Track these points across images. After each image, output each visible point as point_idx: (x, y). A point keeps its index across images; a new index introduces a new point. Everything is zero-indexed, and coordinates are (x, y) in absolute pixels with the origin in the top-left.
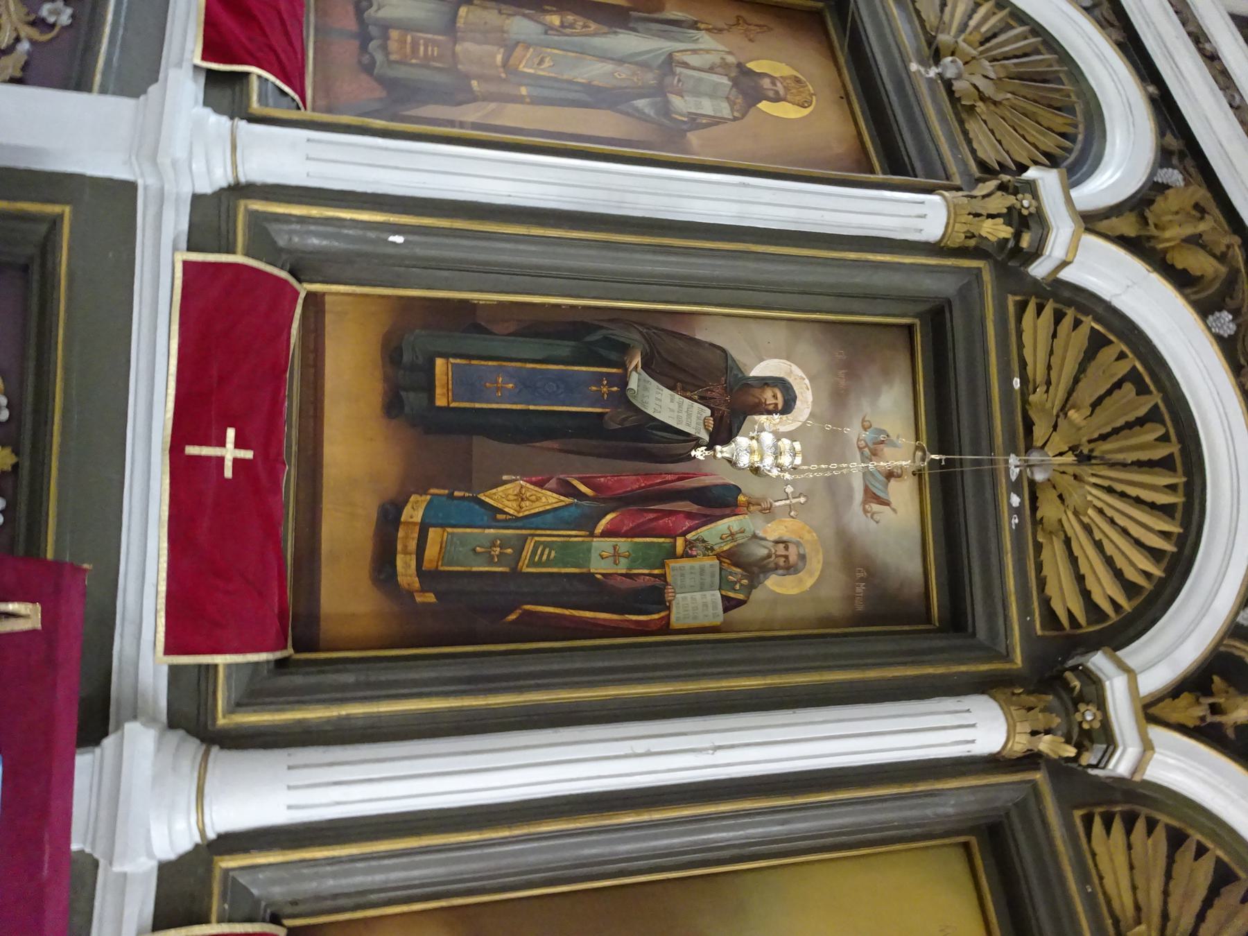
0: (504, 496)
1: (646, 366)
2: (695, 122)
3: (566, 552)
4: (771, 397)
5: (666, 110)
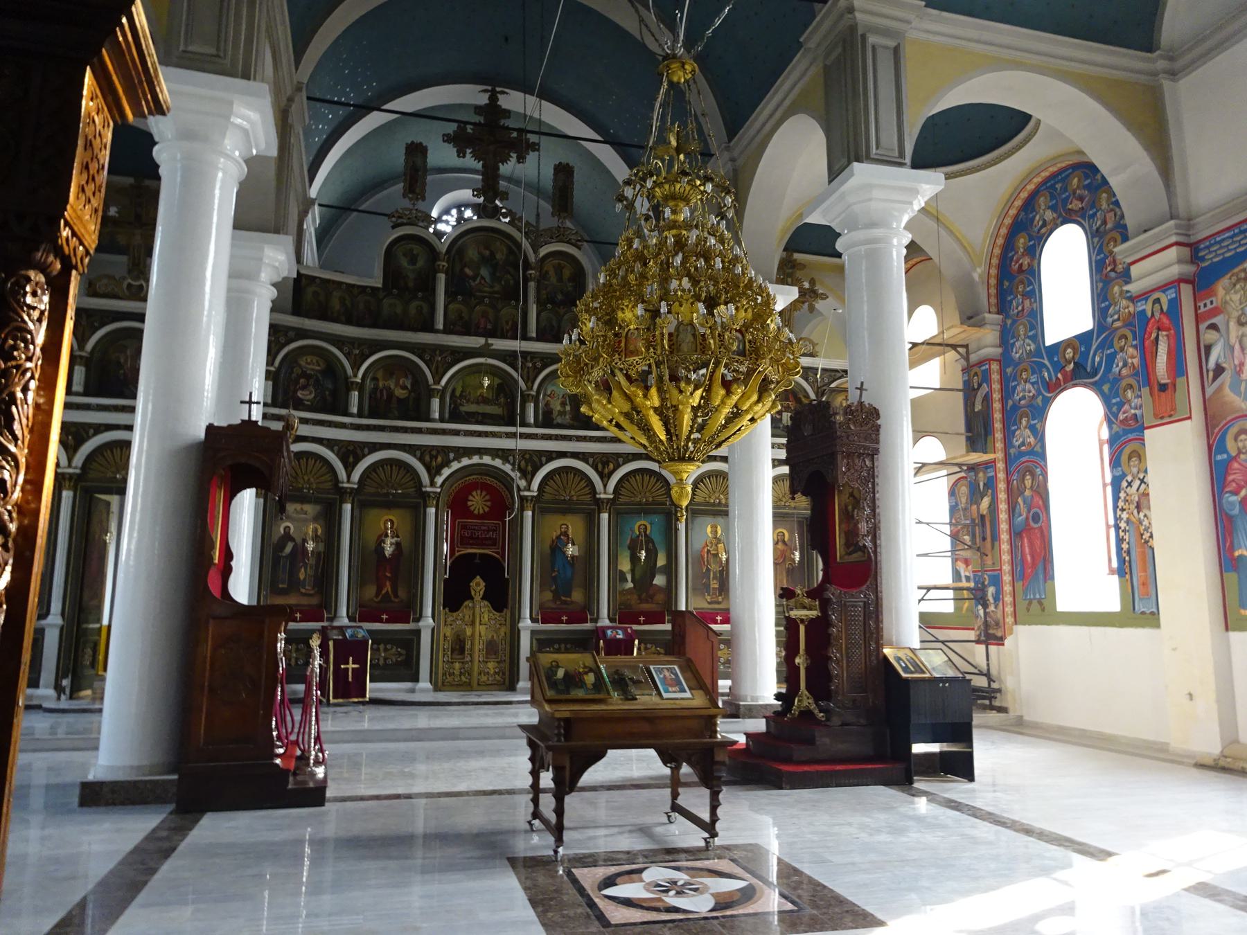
0: (302, 577)
1: (281, 552)
3: (311, 568)
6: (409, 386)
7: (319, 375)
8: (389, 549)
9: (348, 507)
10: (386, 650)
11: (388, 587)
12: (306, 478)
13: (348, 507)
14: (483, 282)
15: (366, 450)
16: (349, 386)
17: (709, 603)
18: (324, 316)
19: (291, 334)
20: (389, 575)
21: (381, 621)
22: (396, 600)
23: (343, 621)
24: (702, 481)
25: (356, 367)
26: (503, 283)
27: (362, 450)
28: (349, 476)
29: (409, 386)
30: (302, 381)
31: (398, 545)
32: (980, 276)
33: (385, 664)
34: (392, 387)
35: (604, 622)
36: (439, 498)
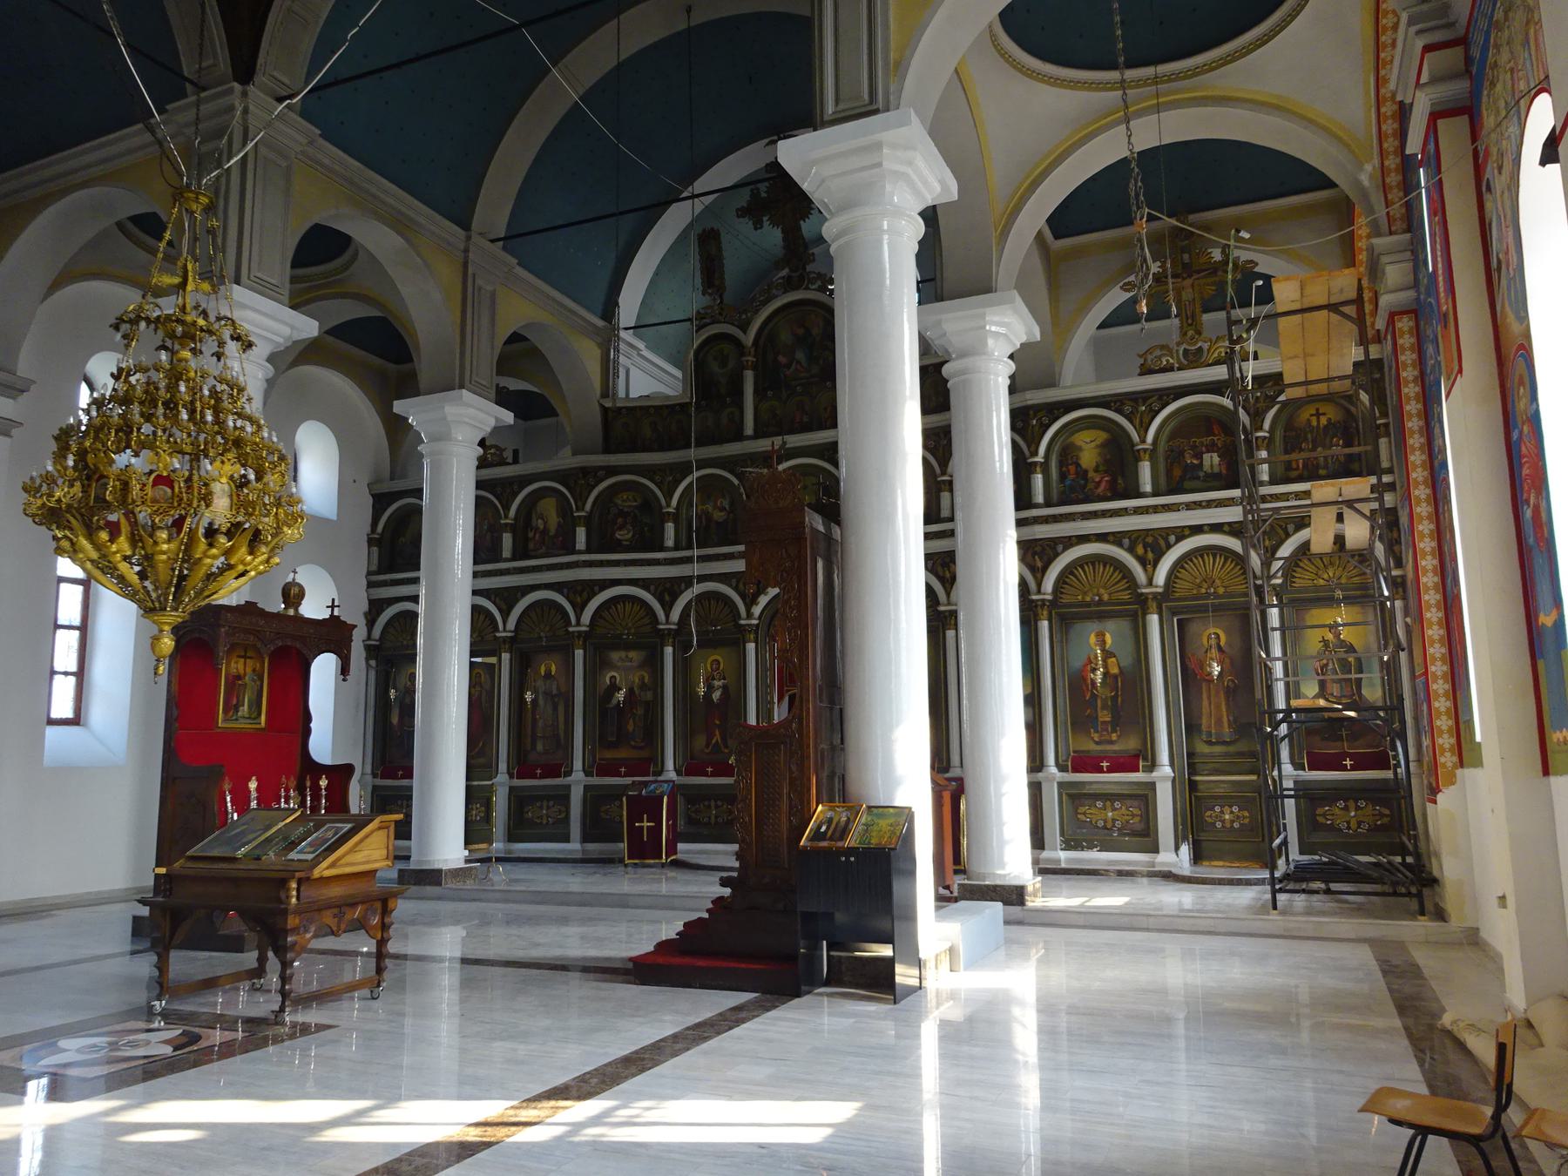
0: (631, 728)
2: (558, 688)
4: (613, 680)
5: (556, 695)
6: (727, 507)
7: (636, 511)
8: (716, 695)
9: (669, 650)
10: (717, 807)
11: (717, 737)
12: (624, 624)
13: (669, 650)
14: (799, 367)
15: (683, 585)
16: (664, 518)
17: (1097, 743)
18: (633, 448)
19: (601, 473)
20: (717, 722)
21: (706, 775)
22: (726, 751)
23: (672, 775)
24: (1072, 573)
25: (669, 496)
26: (821, 362)
27: (680, 586)
28: (667, 616)
29: (727, 507)
30: (620, 520)
31: (725, 687)
32: (1371, 177)
33: (716, 823)
34: (710, 509)
35: (672, 775)
36: (757, 633)
